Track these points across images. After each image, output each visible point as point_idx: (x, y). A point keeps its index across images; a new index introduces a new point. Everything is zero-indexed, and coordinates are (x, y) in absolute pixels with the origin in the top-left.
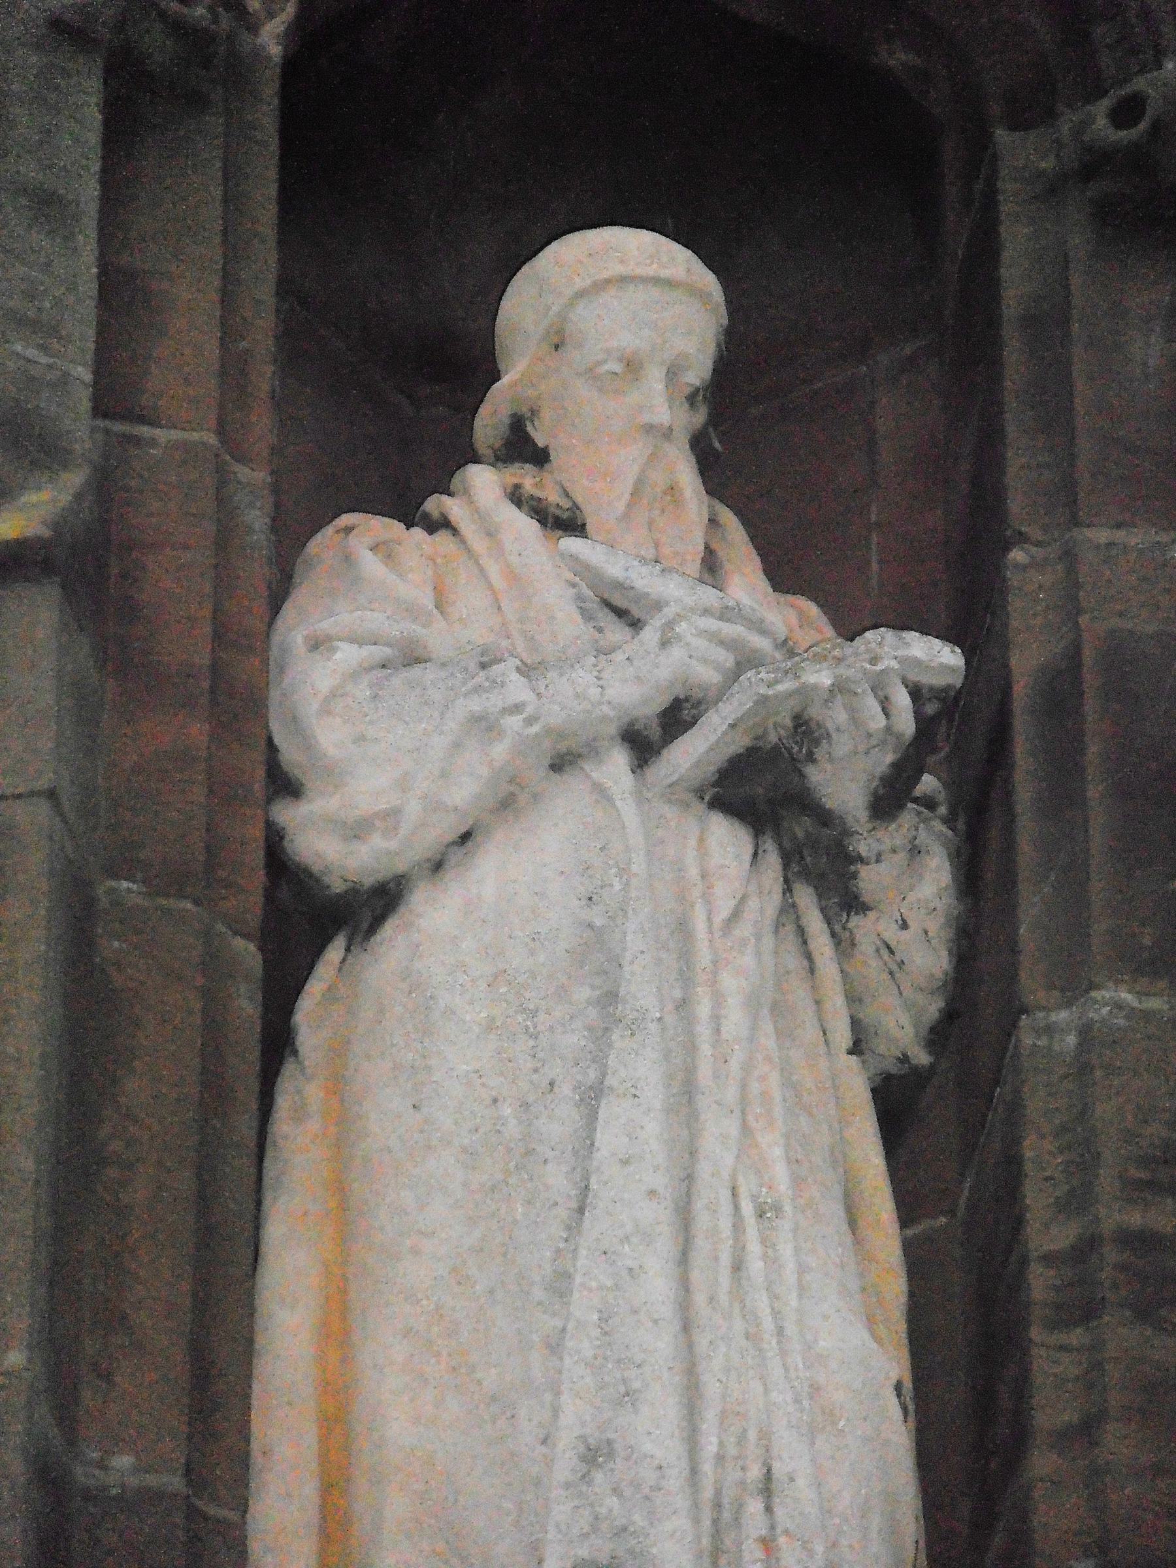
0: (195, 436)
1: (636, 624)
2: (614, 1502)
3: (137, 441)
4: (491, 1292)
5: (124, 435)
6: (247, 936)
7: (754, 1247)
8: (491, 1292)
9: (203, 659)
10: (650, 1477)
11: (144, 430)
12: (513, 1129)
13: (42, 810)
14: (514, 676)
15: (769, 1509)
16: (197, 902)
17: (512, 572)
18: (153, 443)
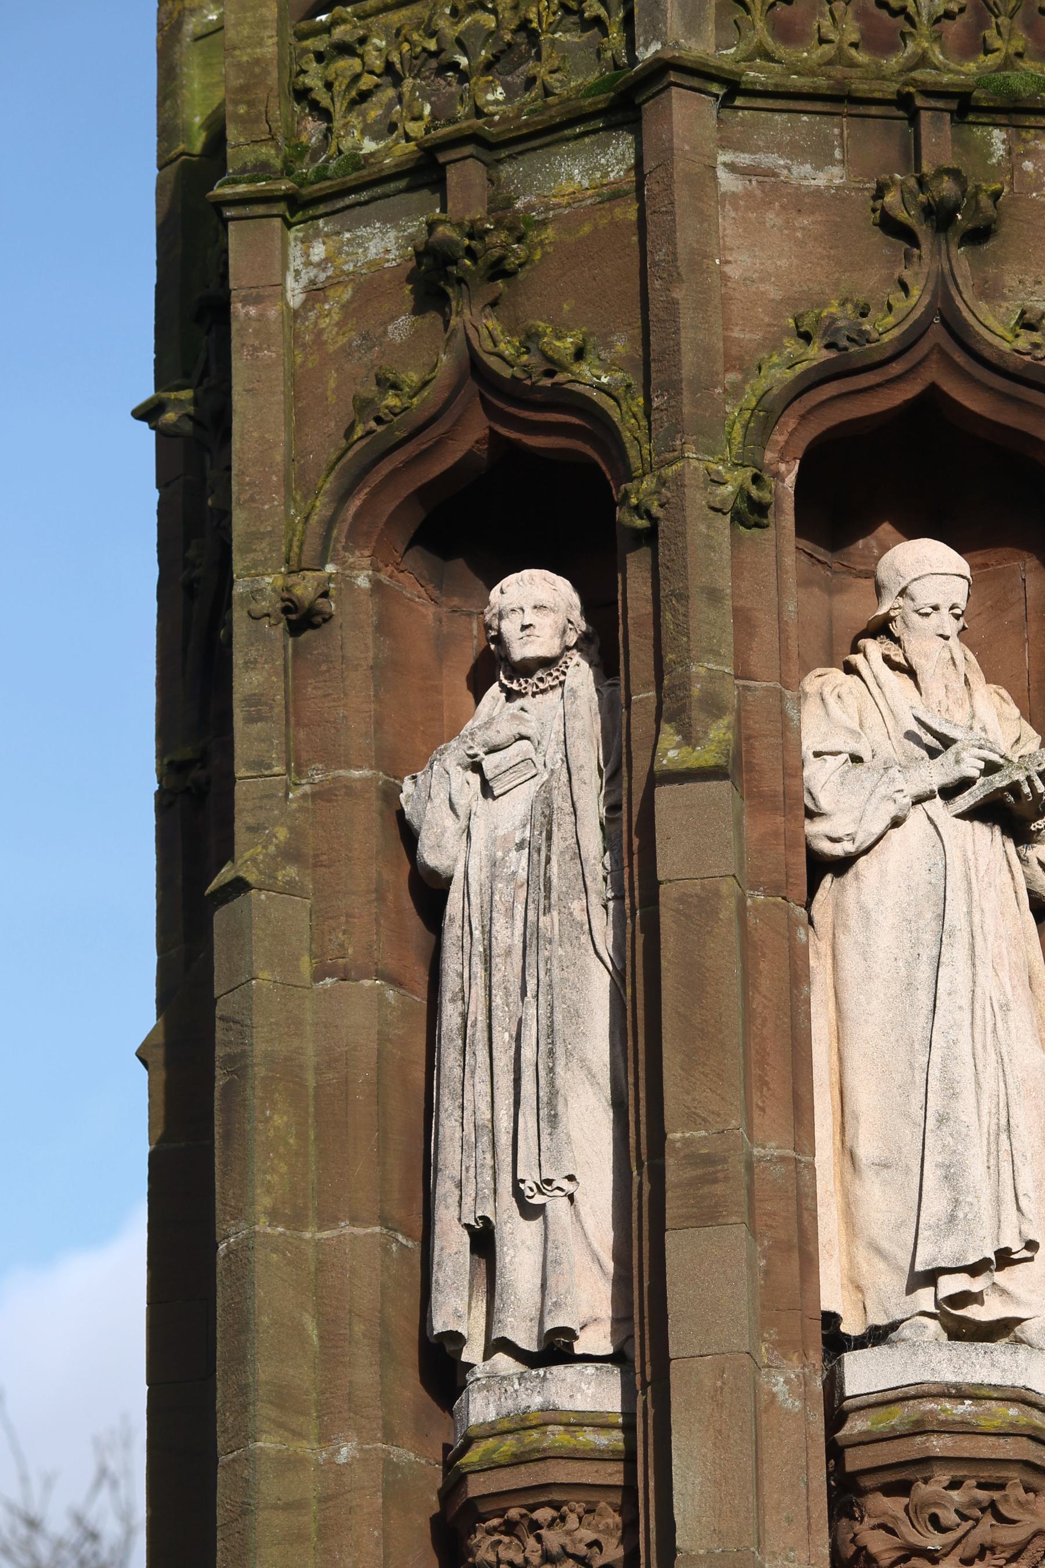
0: (771, 684)
1: (947, 747)
2: (950, 1139)
3: (747, 688)
4: (897, 1041)
5: (743, 686)
6: (801, 906)
7: (999, 1024)
8: (897, 1041)
9: (780, 789)
10: (964, 1130)
11: (752, 683)
12: (903, 972)
13: (731, 881)
14: (898, 775)
15: (1009, 1138)
16: (784, 898)
17: (799, 424)
18: (756, 689)
